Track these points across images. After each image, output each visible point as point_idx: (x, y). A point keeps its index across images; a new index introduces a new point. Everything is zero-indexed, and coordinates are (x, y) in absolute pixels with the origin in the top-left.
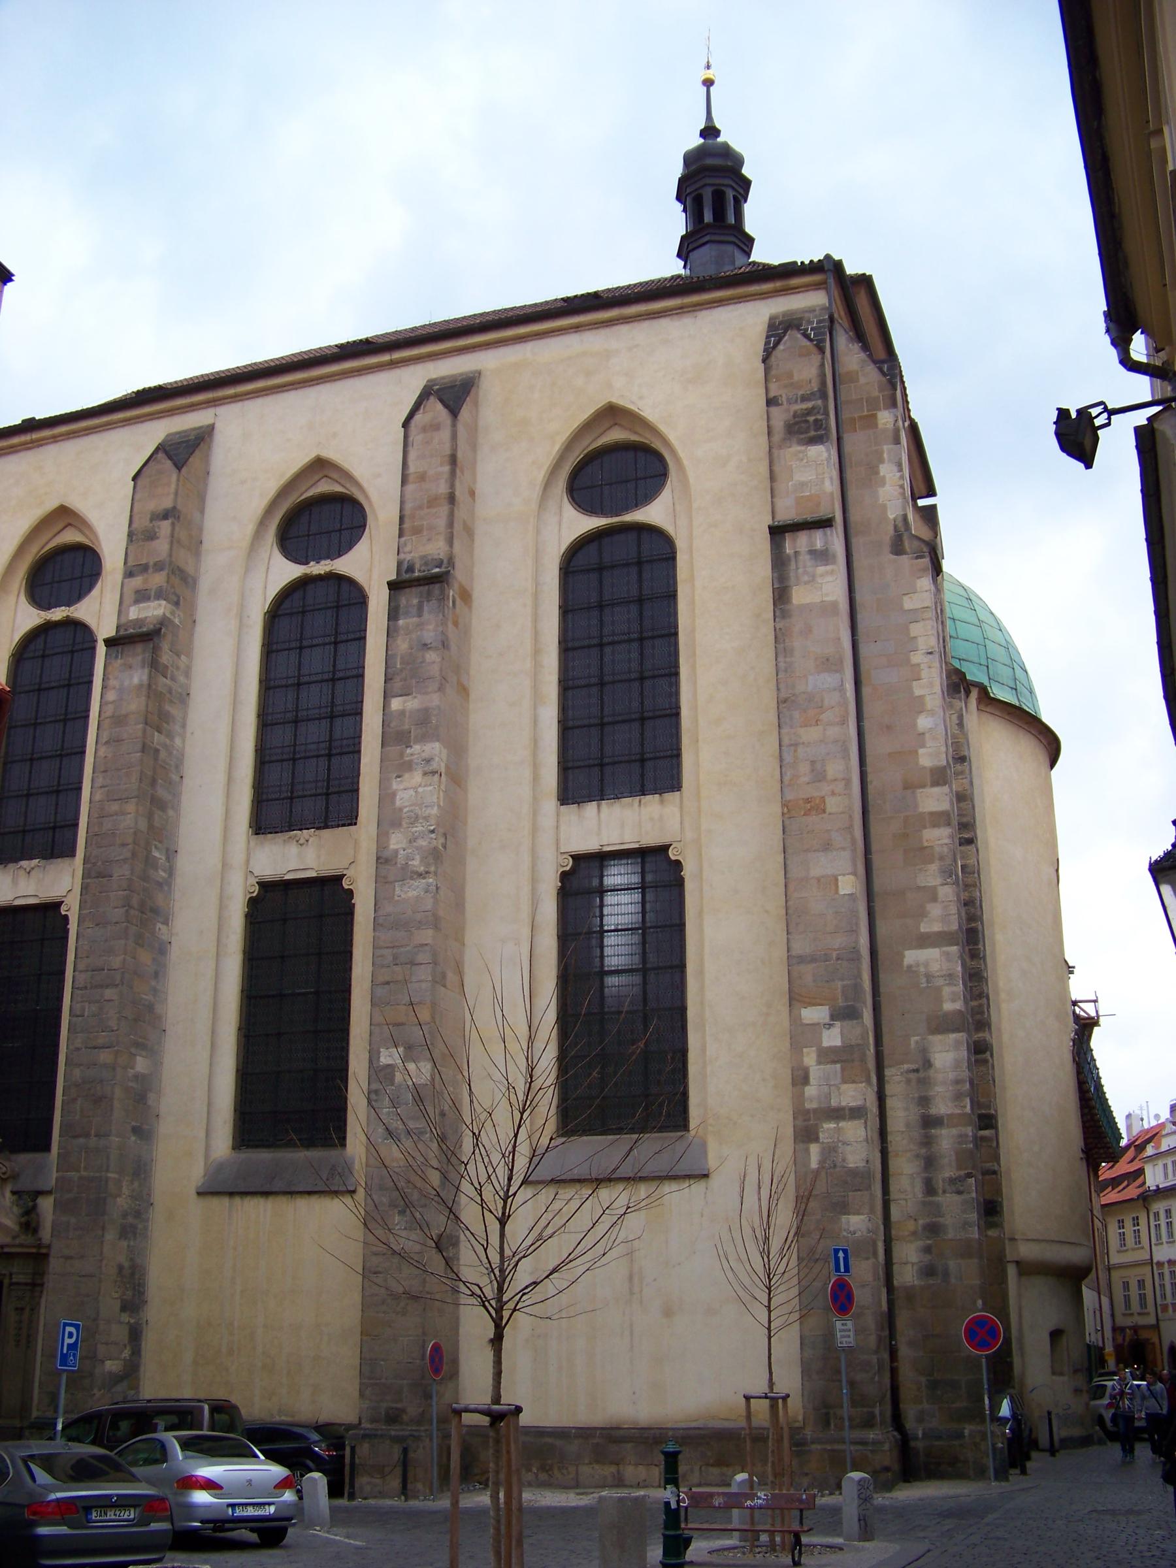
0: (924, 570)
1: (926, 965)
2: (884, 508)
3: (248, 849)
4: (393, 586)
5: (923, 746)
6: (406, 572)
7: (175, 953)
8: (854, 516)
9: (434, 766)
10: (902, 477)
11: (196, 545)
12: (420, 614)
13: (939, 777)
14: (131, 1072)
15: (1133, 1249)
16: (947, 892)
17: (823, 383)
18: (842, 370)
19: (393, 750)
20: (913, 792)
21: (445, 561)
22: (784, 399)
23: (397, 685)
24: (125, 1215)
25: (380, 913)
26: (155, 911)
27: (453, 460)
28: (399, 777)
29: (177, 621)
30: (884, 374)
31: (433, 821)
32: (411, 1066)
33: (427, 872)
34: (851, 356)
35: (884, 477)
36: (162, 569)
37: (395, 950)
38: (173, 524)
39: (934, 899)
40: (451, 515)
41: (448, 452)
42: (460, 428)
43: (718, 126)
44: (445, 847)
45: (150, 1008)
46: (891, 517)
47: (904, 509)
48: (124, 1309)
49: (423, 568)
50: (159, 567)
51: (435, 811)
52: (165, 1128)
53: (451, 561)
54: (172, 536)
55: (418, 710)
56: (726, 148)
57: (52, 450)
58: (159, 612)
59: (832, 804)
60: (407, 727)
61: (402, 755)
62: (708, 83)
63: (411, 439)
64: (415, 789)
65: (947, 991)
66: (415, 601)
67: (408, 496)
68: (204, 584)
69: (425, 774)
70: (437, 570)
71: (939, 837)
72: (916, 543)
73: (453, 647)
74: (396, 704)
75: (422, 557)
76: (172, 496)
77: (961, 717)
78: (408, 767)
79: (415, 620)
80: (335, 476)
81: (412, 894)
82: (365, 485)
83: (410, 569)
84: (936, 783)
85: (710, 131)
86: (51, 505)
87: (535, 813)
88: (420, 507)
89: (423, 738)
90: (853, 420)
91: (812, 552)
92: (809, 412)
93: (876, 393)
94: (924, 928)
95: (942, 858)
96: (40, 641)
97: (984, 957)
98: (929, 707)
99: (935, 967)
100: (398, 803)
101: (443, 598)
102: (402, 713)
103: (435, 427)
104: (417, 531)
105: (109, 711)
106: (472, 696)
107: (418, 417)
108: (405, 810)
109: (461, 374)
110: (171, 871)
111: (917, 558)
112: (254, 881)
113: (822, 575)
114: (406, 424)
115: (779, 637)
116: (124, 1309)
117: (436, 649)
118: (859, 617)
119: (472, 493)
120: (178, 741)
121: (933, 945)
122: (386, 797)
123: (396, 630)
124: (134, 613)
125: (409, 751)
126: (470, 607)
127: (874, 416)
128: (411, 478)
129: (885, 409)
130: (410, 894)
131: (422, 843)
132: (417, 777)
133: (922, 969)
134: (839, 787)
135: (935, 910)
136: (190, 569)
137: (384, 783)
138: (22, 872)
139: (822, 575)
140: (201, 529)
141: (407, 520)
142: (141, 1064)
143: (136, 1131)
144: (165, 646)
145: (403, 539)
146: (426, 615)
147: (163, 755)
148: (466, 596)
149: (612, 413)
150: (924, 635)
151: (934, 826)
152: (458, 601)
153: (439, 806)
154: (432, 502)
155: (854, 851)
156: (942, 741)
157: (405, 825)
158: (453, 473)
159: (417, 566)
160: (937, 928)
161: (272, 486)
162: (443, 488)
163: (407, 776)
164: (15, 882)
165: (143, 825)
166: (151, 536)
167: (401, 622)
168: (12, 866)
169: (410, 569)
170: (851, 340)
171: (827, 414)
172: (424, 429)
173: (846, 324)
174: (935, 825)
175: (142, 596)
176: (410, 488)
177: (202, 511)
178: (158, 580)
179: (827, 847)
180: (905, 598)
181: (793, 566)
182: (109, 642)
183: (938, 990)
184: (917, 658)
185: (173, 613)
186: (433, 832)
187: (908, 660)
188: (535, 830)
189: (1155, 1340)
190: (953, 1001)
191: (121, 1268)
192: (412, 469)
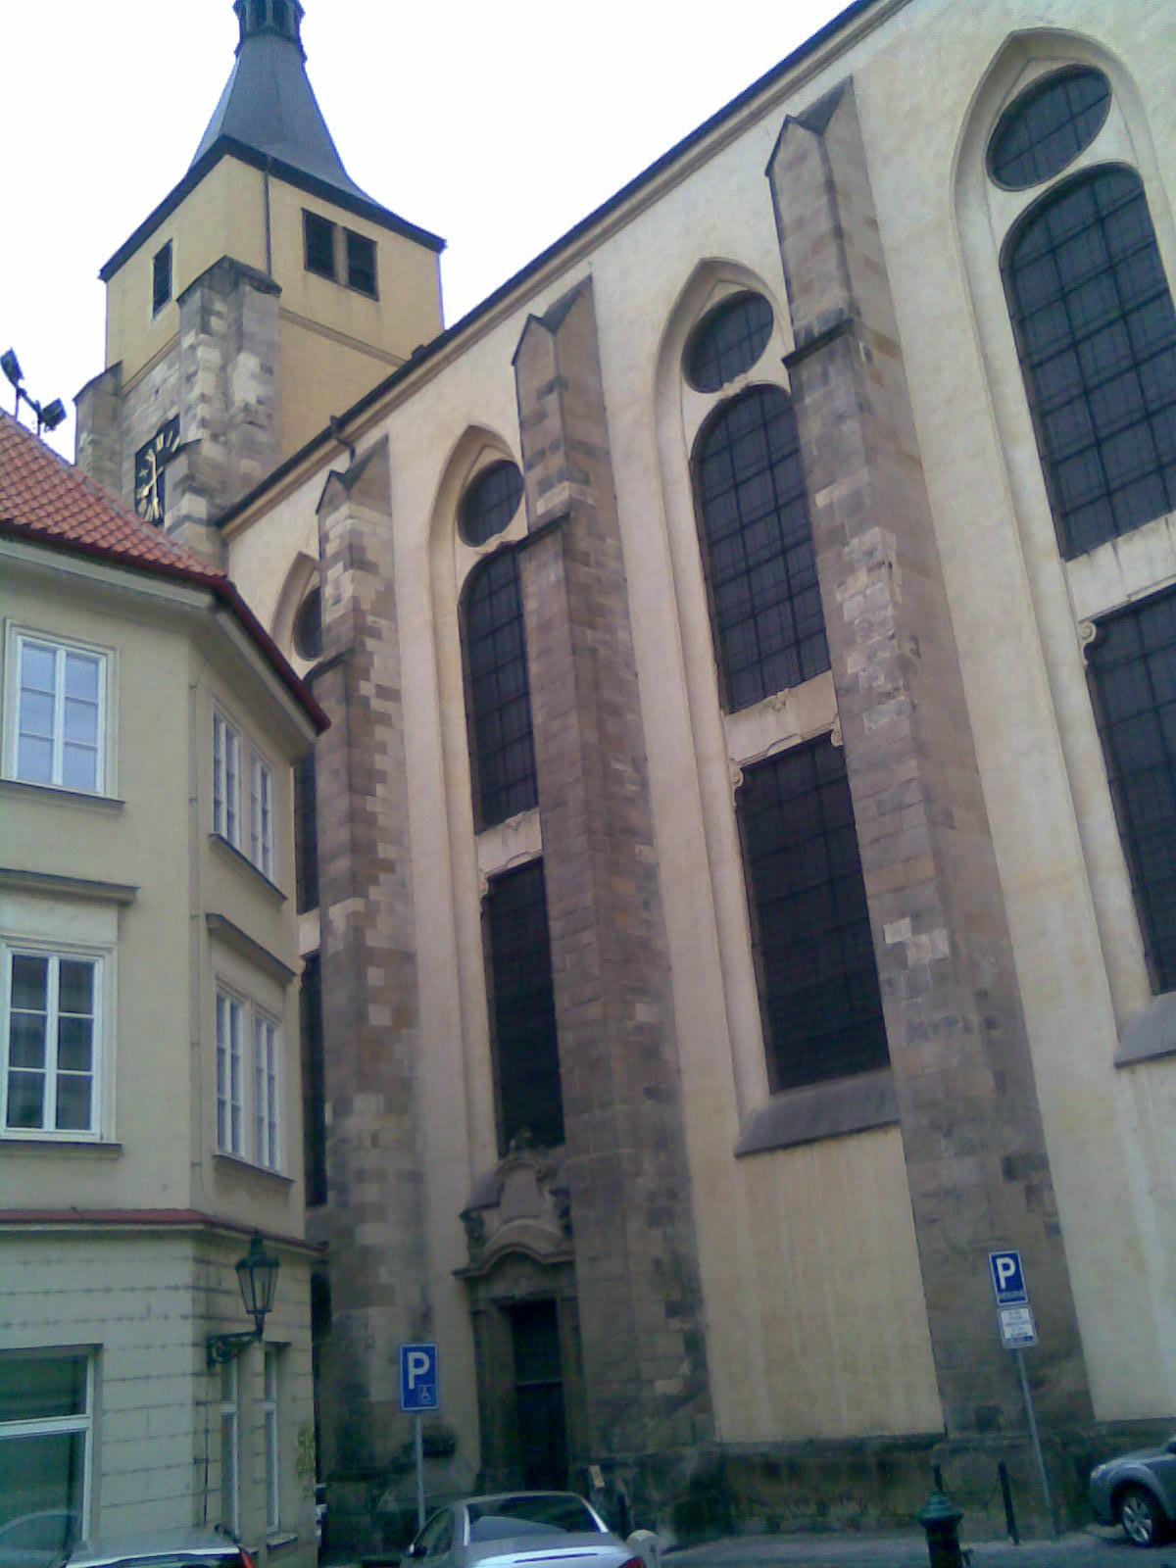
3: (724, 735)
7: (665, 875)
9: (878, 556)
11: (598, 412)
14: (630, 1025)
24: (652, 1197)
26: (631, 832)
27: (830, 186)
28: (840, 585)
29: (590, 501)
32: (924, 938)
33: (897, 689)
36: (558, 449)
38: (561, 397)
40: (842, 251)
41: (822, 180)
42: (834, 149)
44: (919, 656)
45: (645, 944)
48: (673, 1310)
50: (554, 446)
51: (890, 611)
52: (690, 1083)
53: (853, 306)
54: (562, 407)
57: (448, 375)
58: (565, 495)
61: (839, 555)
63: (778, 186)
64: (863, 593)
76: (552, 364)
80: (727, 275)
82: (757, 269)
86: (459, 430)
87: (1033, 581)
89: (860, 528)
96: (484, 581)
100: (846, 616)
103: (801, 158)
104: (807, 288)
106: (926, 463)
108: (856, 622)
110: (644, 784)
112: (735, 769)
114: (769, 172)
116: (673, 1310)
120: (622, 635)
125: (847, 549)
130: (881, 723)
131: (884, 655)
132: (863, 577)
138: (509, 831)
140: (600, 394)
142: (644, 1013)
143: (650, 1093)
145: (794, 305)
146: (834, 381)
147: (603, 652)
148: (890, 346)
152: (875, 353)
153: (895, 604)
154: (817, 246)
158: (833, 203)
162: (825, 225)
163: (850, 581)
164: (505, 842)
166: (541, 416)
168: (500, 827)
176: (789, 242)
177: (598, 373)
178: (557, 461)
185: (583, 493)
188: (1037, 603)
191: (657, 1263)
192: (787, 217)
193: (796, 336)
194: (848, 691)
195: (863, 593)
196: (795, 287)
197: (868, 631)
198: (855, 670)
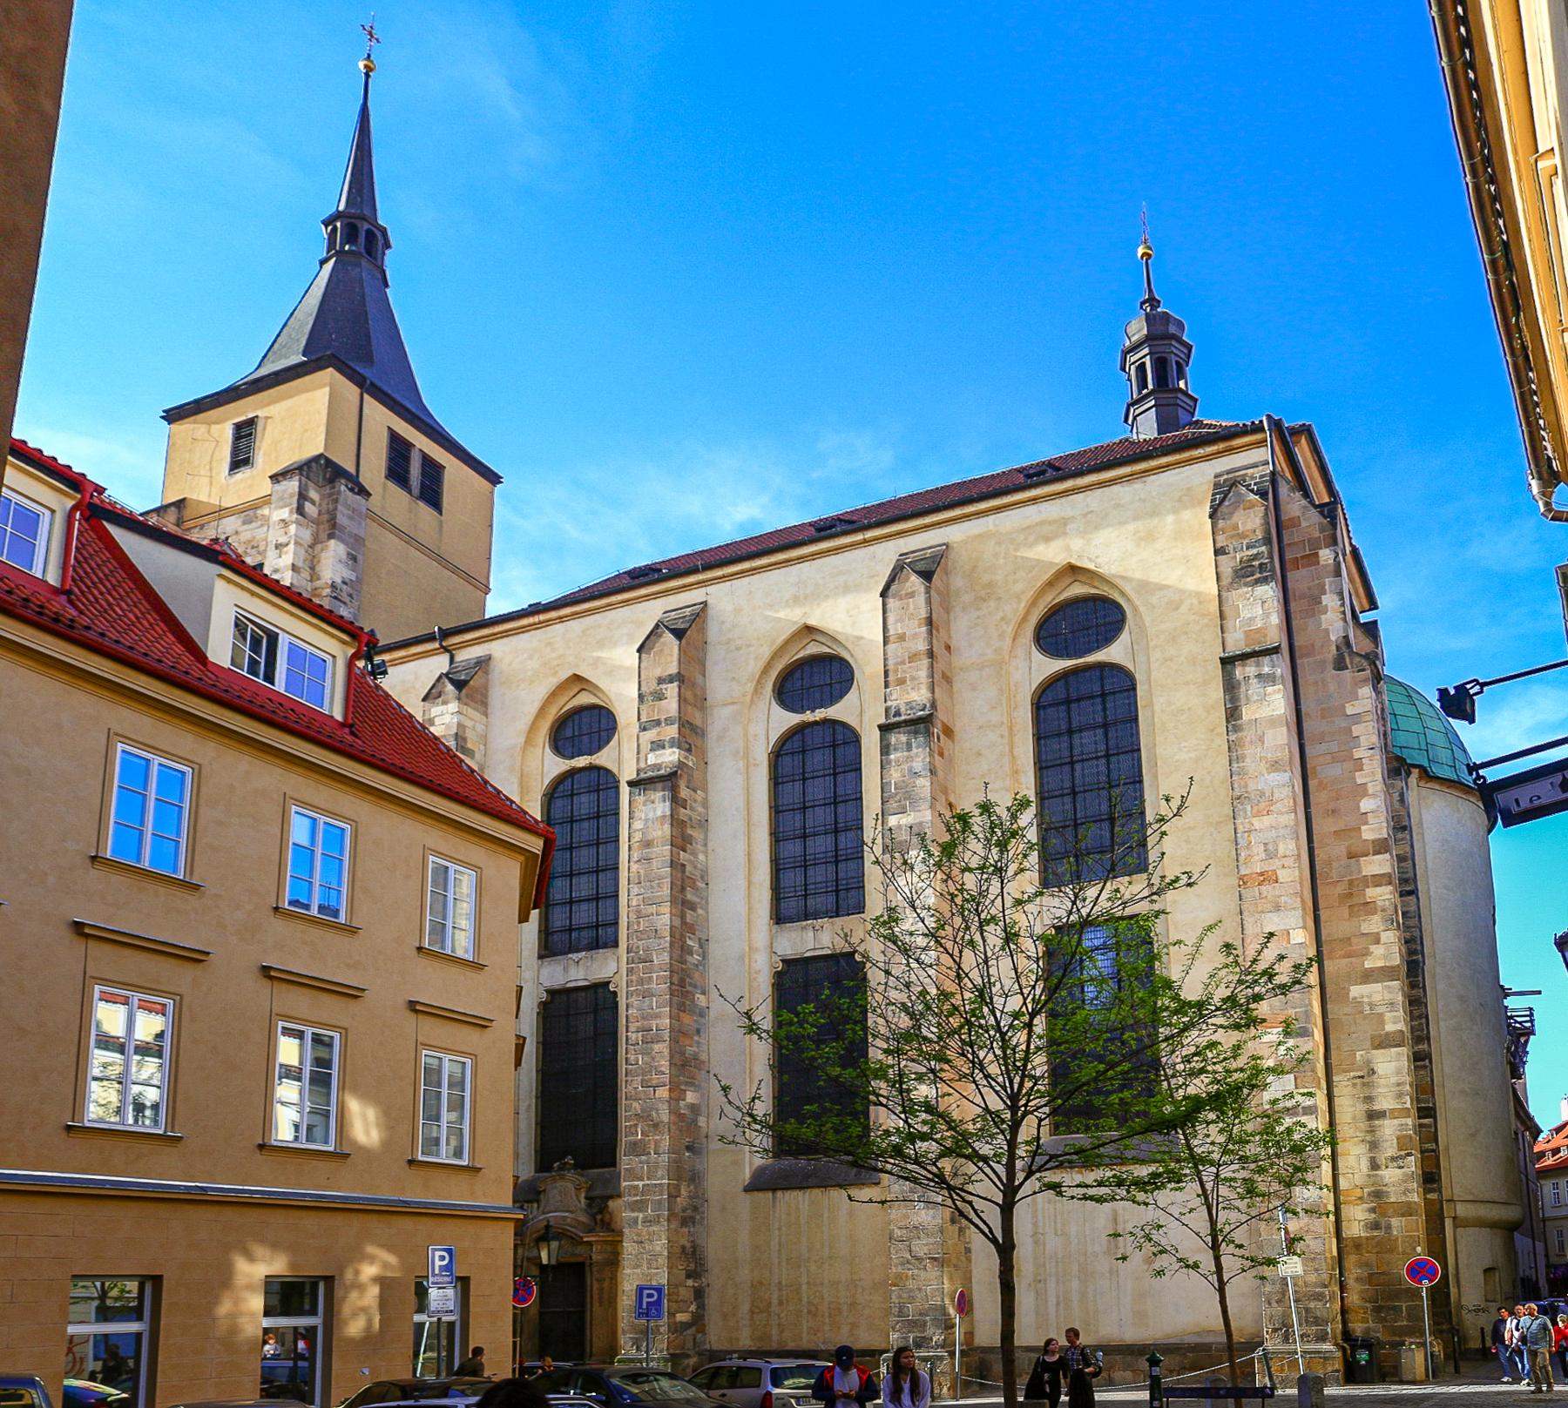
1: (1370, 997)
2: (1327, 631)
4: (885, 729)
5: (1366, 823)
8: (1299, 641)
13: (1380, 847)
17: (1268, 532)
23: (893, 805)
27: (930, 622)
34: (1294, 505)
39: (1377, 942)
47: (1346, 629)
59: (1283, 875)
67: (889, 654)
68: (713, 731)
71: (1384, 895)
73: (940, 773)
77: (1402, 795)
83: (897, 714)
92: (1255, 557)
93: (1317, 534)
97: (1424, 988)
99: (1377, 998)
101: (928, 734)
102: (899, 827)
103: (911, 595)
104: (901, 682)
105: (637, 837)
118: (1305, 725)
119: (948, 648)
124: (652, 759)
127: (1317, 554)
134: (1290, 862)
136: (698, 722)
144: (682, 784)
149: (1073, 571)
150: (1367, 734)
154: (913, 657)
155: (1304, 909)
158: (930, 633)
159: (903, 710)
160: (1380, 964)
161: (766, 652)
165: (677, 922)
169: (897, 714)
170: (1292, 490)
171: (1271, 557)
175: (657, 745)
176: (891, 647)
179: (1277, 908)
181: (1243, 689)
182: (631, 784)
183: (1381, 1015)
192: (891, 632)
193: (887, 710)
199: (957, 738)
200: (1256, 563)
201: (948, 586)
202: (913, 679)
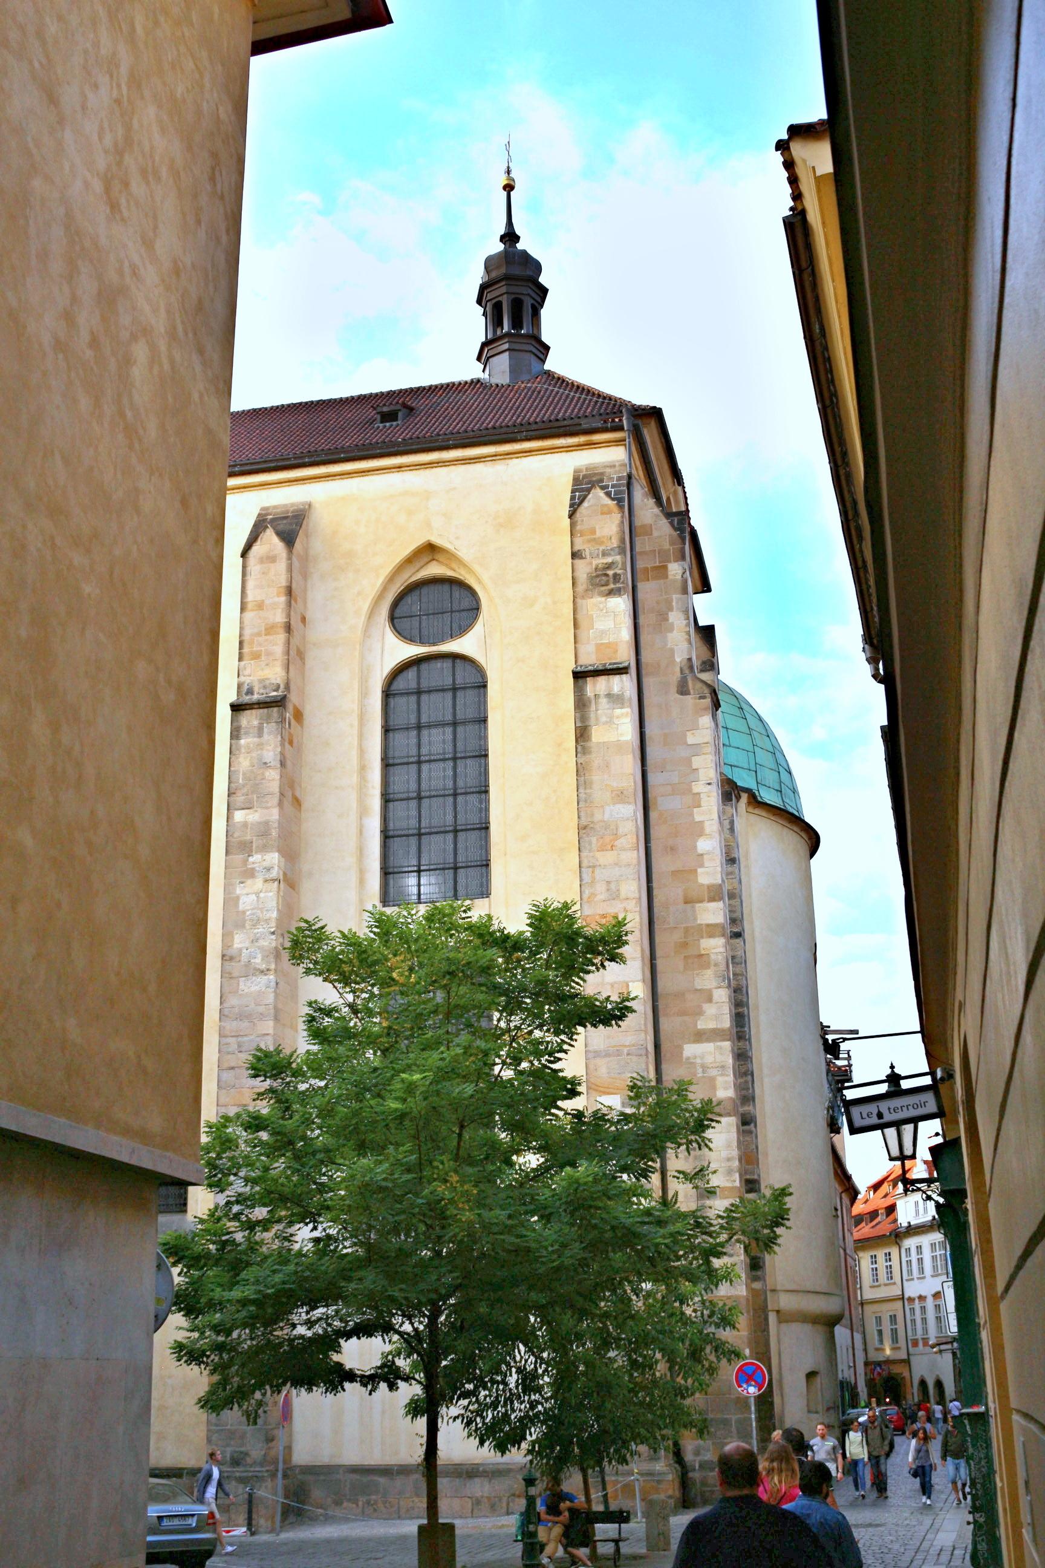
0: (706, 709)
1: (702, 1058)
2: (672, 651)
4: (236, 708)
5: (702, 866)
6: (247, 694)
10: (688, 625)
12: (260, 734)
13: (715, 894)
15: (886, 1285)
16: (722, 995)
18: (638, 523)
19: (238, 858)
20: (693, 907)
21: (282, 686)
22: (587, 553)
23: (239, 799)
25: (225, 1005)
27: (289, 591)
30: (676, 529)
31: (273, 924)
33: (268, 970)
34: (647, 510)
35: (672, 624)
37: (240, 1039)
39: (710, 1000)
42: (294, 559)
43: (518, 233)
46: (678, 660)
47: (690, 652)
49: (262, 691)
51: (275, 915)
55: (260, 823)
56: (525, 254)
60: (248, 838)
62: (509, 188)
63: (248, 569)
64: (257, 894)
65: (720, 1080)
66: (256, 723)
67: (246, 622)
69: (266, 881)
70: (275, 694)
71: (716, 947)
72: (699, 685)
74: (239, 816)
75: (261, 681)
78: (251, 874)
79: (256, 740)
81: (254, 988)
83: (250, 692)
84: (712, 899)
85: (510, 237)
88: (259, 634)
90: (646, 570)
91: (609, 696)
94: (701, 1025)
95: (716, 965)
98: (707, 830)
99: (709, 1059)
100: (241, 907)
102: (245, 825)
103: (272, 559)
104: (256, 656)
107: (256, 549)
109: (292, 505)
111: (701, 698)
113: (618, 717)
115: (581, 770)
117: (274, 768)
121: (708, 1040)
122: (231, 901)
123: (239, 749)
126: (302, 727)
127: (665, 568)
128: (250, 606)
129: (675, 561)
131: (264, 943)
132: (258, 883)
133: (698, 1061)
135: (710, 1010)
137: (228, 888)
139: (618, 717)
141: (246, 645)
145: (242, 663)
146: (266, 736)
151: (710, 937)
154: (270, 630)
156: (719, 863)
157: (248, 927)
158: (289, 604)
159: (256, 689)
160: (712, 1025)
163: (249, 882)
167: (242, 742)
169: (250, 692)
170: (645, 495)
171: (624, 568)
172: (261, 560)
173: (644, 482)
174: (711, 936)
176: (248, 615)
180: (688, 734)
183: (712, 1080)
184: (698, 787)
186: (273, 933)
187: (690, 790)
189: (906, 1374)
190: (726, 1089)
192: (250, 597)
193: (240, 686)
194: (231, 959)
195: (257, 894)
196: (246, 650)
197: (257, 922)
198: (239, 946)
199: (306, 722)
200: (611, 573)
201: (306, 550)
202: (269, 654)
